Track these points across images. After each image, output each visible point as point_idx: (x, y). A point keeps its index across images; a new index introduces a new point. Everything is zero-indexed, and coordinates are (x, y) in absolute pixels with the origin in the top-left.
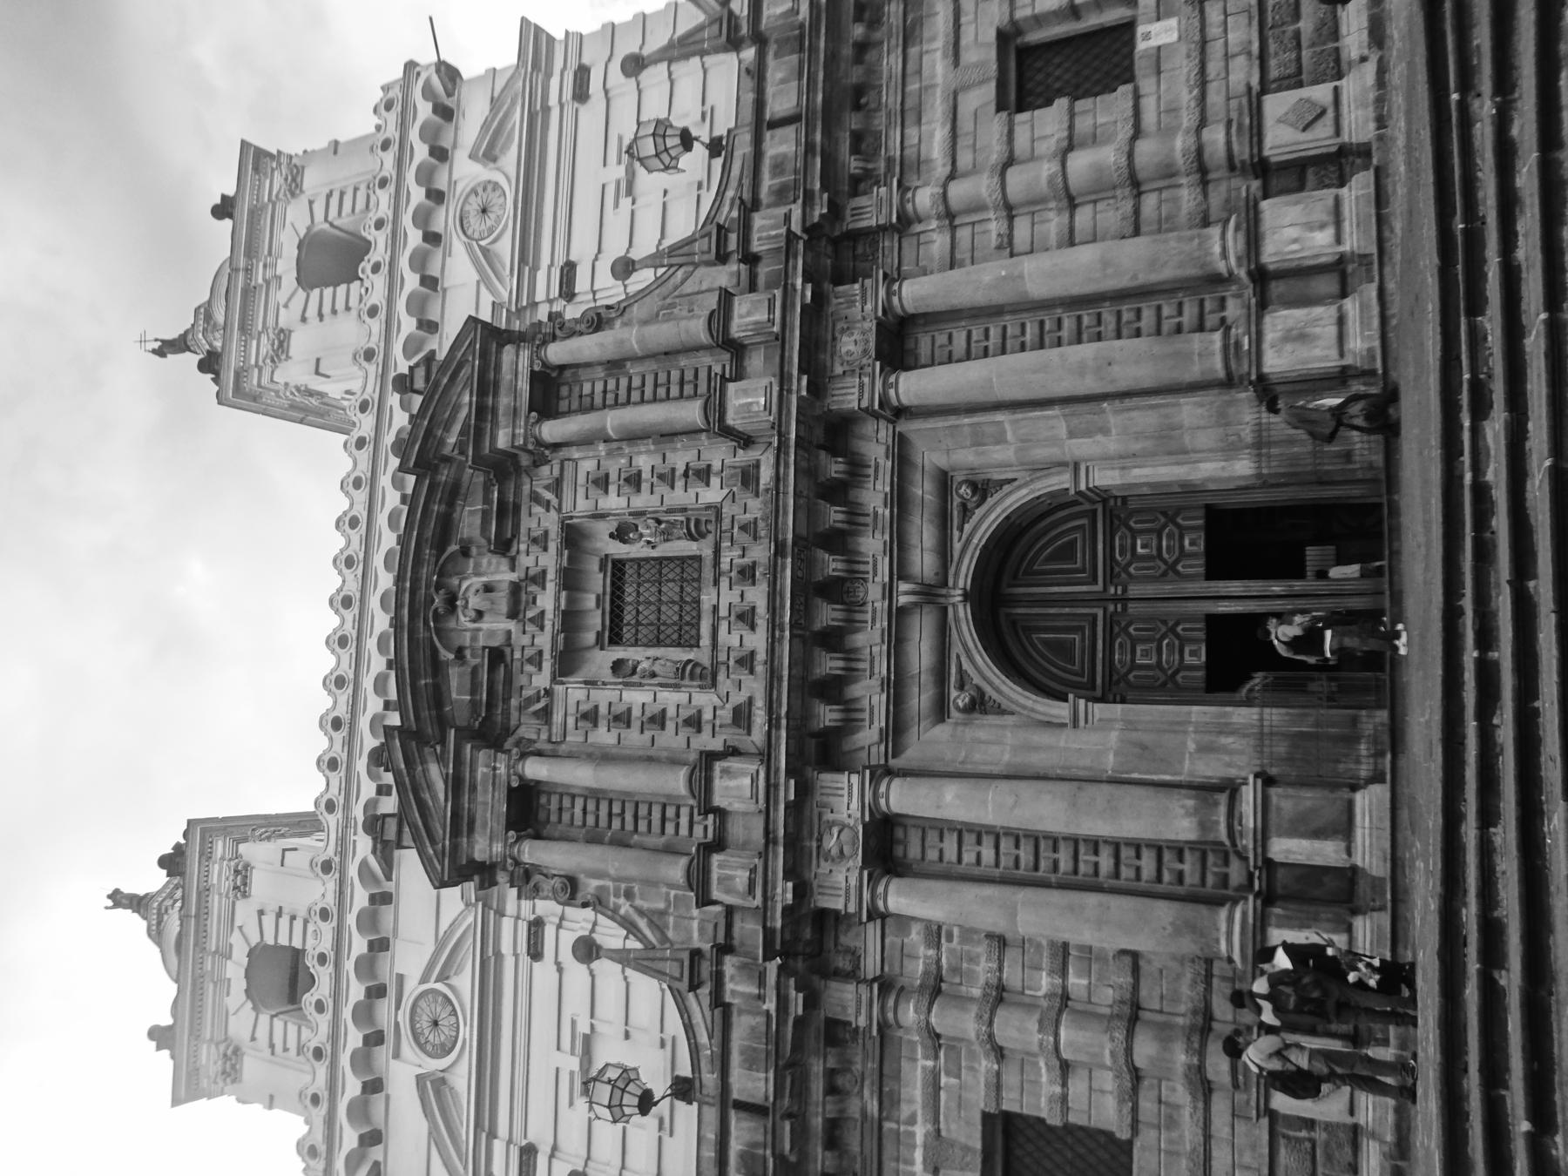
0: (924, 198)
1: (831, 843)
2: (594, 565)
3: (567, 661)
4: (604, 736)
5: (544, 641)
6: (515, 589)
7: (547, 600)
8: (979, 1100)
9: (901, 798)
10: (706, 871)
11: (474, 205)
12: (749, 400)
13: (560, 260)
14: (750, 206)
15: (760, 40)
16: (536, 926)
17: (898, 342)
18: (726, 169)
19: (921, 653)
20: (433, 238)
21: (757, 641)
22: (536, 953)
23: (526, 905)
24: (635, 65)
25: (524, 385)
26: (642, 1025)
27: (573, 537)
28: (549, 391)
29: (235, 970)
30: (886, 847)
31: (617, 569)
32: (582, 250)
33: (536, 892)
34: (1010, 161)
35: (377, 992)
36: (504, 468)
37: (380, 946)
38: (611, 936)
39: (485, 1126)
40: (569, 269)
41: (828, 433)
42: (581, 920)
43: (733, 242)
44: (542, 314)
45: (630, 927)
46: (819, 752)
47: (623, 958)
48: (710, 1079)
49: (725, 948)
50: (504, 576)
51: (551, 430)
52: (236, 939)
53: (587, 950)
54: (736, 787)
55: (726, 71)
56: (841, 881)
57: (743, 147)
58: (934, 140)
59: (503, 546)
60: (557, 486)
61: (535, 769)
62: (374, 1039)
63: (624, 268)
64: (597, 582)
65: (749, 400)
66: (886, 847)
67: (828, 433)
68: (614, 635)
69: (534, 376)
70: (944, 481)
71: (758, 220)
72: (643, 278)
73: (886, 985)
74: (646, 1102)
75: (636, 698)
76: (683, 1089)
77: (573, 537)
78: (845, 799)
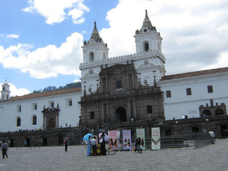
0: (141, 102)
1: (105, 102)
2: (121, 80)
3: (115, 79)
4: (110, 84)
5: (115, 77)
6: (118, 74)
7: (118, 77)
8: (94, 111)
9: (107, 106)
10: (103, 94)
11: (147, 62)
12: (128, 92)
13: (141, 73)
14: (142, 89)
15: (155, 87)
16: (98, 80)
17: (131, 101)
18: (145, 86)
19: (116, 104)
20: (144, 59)
21: (116, 94)
22: (97, 80)
23: (99, 79)
24: (155, 77)
25: (130, 73)
26: (94, 90)
27: (122, 78)
28: (130, 75)
29: (91, 51)
30: (105, 105)
31: (121, 81)
32: (142, 74)
33: (100, 80)
34: (143, 107)
35: (92, 67)
36: (125, 72)
37: (95, 67)
38: (99, 87)
39: (86, 79)
40: (140, 74)
41: (126, 98)
42: (99, 84)
43: (140, 88)
44: (137, 72)
45: (99, 88)
46: (109, 100)
47: (98, 87)
48: (92, 95)
49: (99, 95)
50: (119, 73)
51: (128, 76)
52: (93, 50)
53: (97, 85)
54: (107, 95)
55: (152, 85)
56: (103, 103)
57: (147, 87)
58: (145, 101)
59: (121, 73)
60: (125, 76)
61: (107, 79)
62: (89, 68)
63: (140, 79)
64: (120, 80)
65: (128, 92)
66: (105, 105)
67: (126, 98)
68: (117, 82)
69: (131, 74)
70: (126, 104)
71: (141, 90)
72: (139, 81)
73: (99, 105)
74: (90, 92)
75: (112, 86)
76: (92, 93)
77: (122, 78)
78: (107, 102)
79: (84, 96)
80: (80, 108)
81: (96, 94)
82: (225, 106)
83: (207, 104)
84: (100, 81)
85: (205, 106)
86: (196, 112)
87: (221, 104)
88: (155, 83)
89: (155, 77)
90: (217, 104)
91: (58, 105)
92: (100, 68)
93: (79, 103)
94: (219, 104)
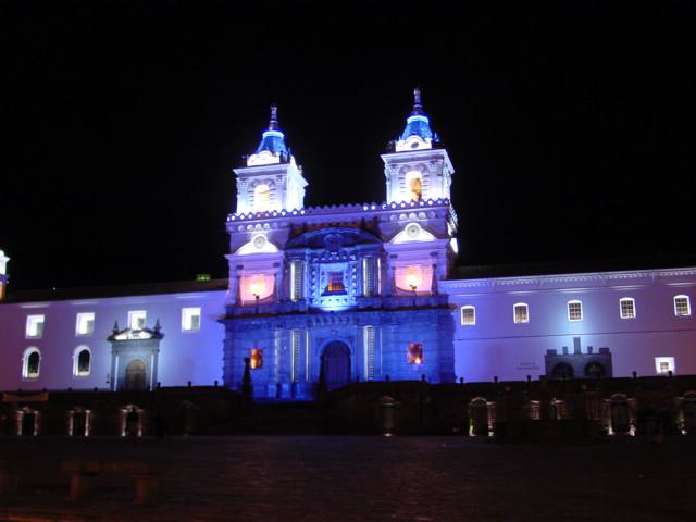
16: (276, 265)
38: (278, 284)
79: (233, 302)
80: (223, 336)
81: (271, 300)
82: (610, 355)
83: (565, 349)
84: (282, 264)
85: (560, 352)
86: (537, 365)
87: (601, 349)
88: (435, 287)
89: (435, 266)
90: (590, 349)
91: (158, 324)
92: (288, 229)
93: (220, 321)
94: (596, 351)
